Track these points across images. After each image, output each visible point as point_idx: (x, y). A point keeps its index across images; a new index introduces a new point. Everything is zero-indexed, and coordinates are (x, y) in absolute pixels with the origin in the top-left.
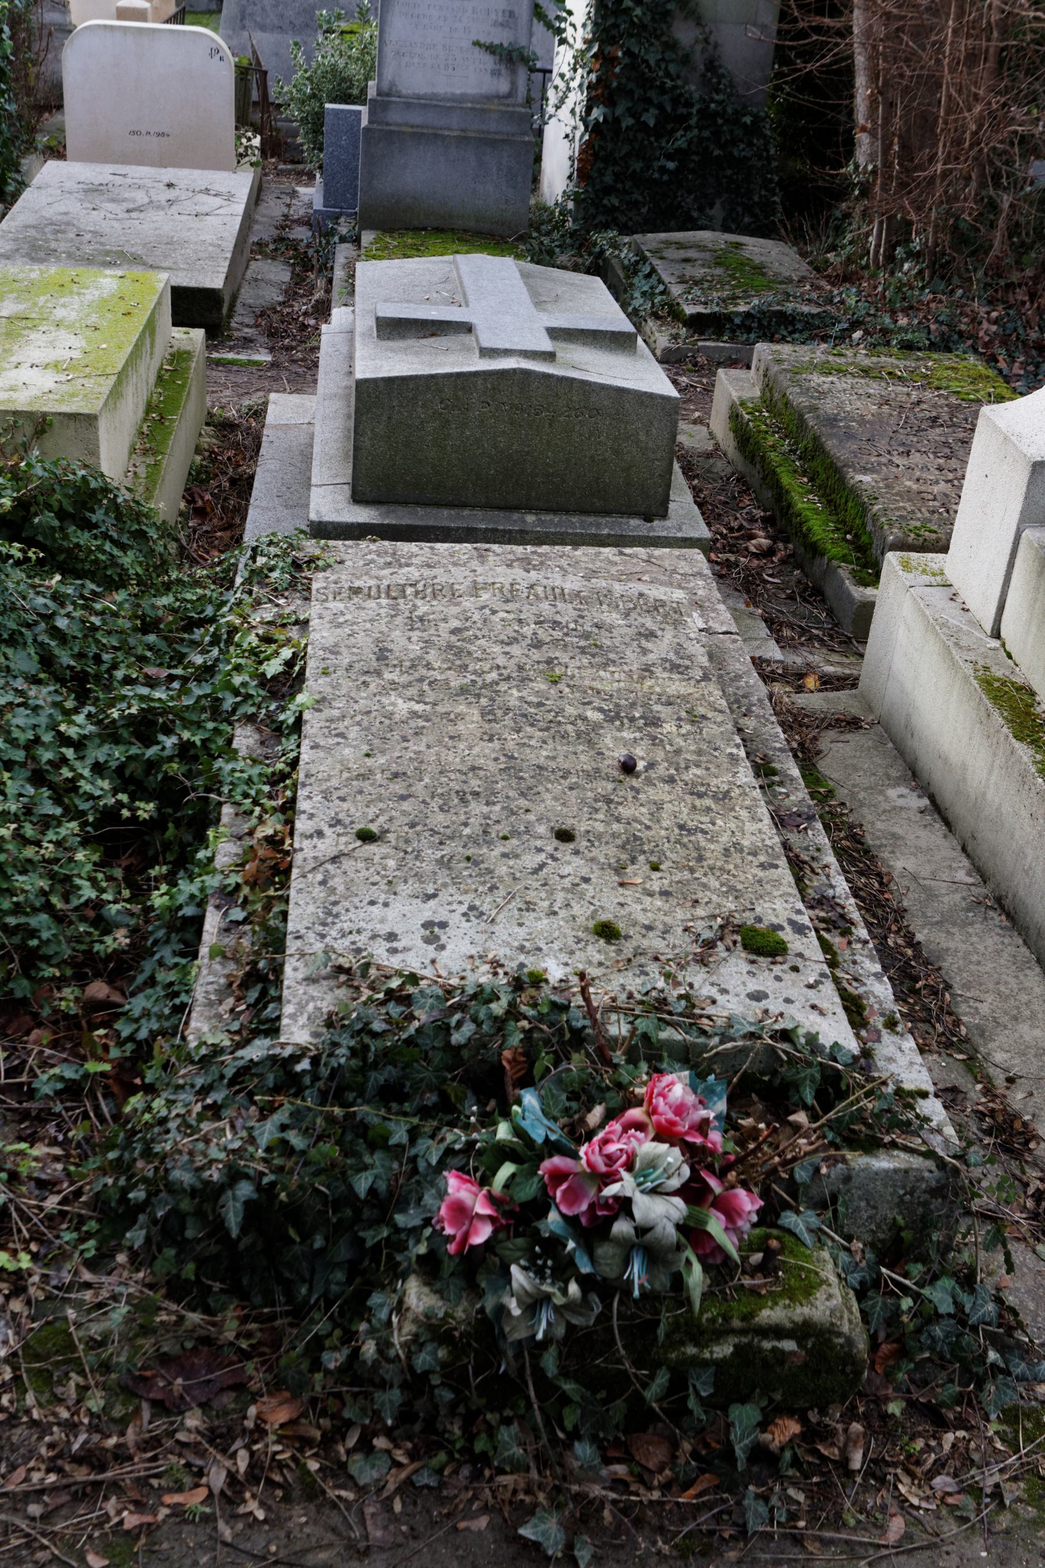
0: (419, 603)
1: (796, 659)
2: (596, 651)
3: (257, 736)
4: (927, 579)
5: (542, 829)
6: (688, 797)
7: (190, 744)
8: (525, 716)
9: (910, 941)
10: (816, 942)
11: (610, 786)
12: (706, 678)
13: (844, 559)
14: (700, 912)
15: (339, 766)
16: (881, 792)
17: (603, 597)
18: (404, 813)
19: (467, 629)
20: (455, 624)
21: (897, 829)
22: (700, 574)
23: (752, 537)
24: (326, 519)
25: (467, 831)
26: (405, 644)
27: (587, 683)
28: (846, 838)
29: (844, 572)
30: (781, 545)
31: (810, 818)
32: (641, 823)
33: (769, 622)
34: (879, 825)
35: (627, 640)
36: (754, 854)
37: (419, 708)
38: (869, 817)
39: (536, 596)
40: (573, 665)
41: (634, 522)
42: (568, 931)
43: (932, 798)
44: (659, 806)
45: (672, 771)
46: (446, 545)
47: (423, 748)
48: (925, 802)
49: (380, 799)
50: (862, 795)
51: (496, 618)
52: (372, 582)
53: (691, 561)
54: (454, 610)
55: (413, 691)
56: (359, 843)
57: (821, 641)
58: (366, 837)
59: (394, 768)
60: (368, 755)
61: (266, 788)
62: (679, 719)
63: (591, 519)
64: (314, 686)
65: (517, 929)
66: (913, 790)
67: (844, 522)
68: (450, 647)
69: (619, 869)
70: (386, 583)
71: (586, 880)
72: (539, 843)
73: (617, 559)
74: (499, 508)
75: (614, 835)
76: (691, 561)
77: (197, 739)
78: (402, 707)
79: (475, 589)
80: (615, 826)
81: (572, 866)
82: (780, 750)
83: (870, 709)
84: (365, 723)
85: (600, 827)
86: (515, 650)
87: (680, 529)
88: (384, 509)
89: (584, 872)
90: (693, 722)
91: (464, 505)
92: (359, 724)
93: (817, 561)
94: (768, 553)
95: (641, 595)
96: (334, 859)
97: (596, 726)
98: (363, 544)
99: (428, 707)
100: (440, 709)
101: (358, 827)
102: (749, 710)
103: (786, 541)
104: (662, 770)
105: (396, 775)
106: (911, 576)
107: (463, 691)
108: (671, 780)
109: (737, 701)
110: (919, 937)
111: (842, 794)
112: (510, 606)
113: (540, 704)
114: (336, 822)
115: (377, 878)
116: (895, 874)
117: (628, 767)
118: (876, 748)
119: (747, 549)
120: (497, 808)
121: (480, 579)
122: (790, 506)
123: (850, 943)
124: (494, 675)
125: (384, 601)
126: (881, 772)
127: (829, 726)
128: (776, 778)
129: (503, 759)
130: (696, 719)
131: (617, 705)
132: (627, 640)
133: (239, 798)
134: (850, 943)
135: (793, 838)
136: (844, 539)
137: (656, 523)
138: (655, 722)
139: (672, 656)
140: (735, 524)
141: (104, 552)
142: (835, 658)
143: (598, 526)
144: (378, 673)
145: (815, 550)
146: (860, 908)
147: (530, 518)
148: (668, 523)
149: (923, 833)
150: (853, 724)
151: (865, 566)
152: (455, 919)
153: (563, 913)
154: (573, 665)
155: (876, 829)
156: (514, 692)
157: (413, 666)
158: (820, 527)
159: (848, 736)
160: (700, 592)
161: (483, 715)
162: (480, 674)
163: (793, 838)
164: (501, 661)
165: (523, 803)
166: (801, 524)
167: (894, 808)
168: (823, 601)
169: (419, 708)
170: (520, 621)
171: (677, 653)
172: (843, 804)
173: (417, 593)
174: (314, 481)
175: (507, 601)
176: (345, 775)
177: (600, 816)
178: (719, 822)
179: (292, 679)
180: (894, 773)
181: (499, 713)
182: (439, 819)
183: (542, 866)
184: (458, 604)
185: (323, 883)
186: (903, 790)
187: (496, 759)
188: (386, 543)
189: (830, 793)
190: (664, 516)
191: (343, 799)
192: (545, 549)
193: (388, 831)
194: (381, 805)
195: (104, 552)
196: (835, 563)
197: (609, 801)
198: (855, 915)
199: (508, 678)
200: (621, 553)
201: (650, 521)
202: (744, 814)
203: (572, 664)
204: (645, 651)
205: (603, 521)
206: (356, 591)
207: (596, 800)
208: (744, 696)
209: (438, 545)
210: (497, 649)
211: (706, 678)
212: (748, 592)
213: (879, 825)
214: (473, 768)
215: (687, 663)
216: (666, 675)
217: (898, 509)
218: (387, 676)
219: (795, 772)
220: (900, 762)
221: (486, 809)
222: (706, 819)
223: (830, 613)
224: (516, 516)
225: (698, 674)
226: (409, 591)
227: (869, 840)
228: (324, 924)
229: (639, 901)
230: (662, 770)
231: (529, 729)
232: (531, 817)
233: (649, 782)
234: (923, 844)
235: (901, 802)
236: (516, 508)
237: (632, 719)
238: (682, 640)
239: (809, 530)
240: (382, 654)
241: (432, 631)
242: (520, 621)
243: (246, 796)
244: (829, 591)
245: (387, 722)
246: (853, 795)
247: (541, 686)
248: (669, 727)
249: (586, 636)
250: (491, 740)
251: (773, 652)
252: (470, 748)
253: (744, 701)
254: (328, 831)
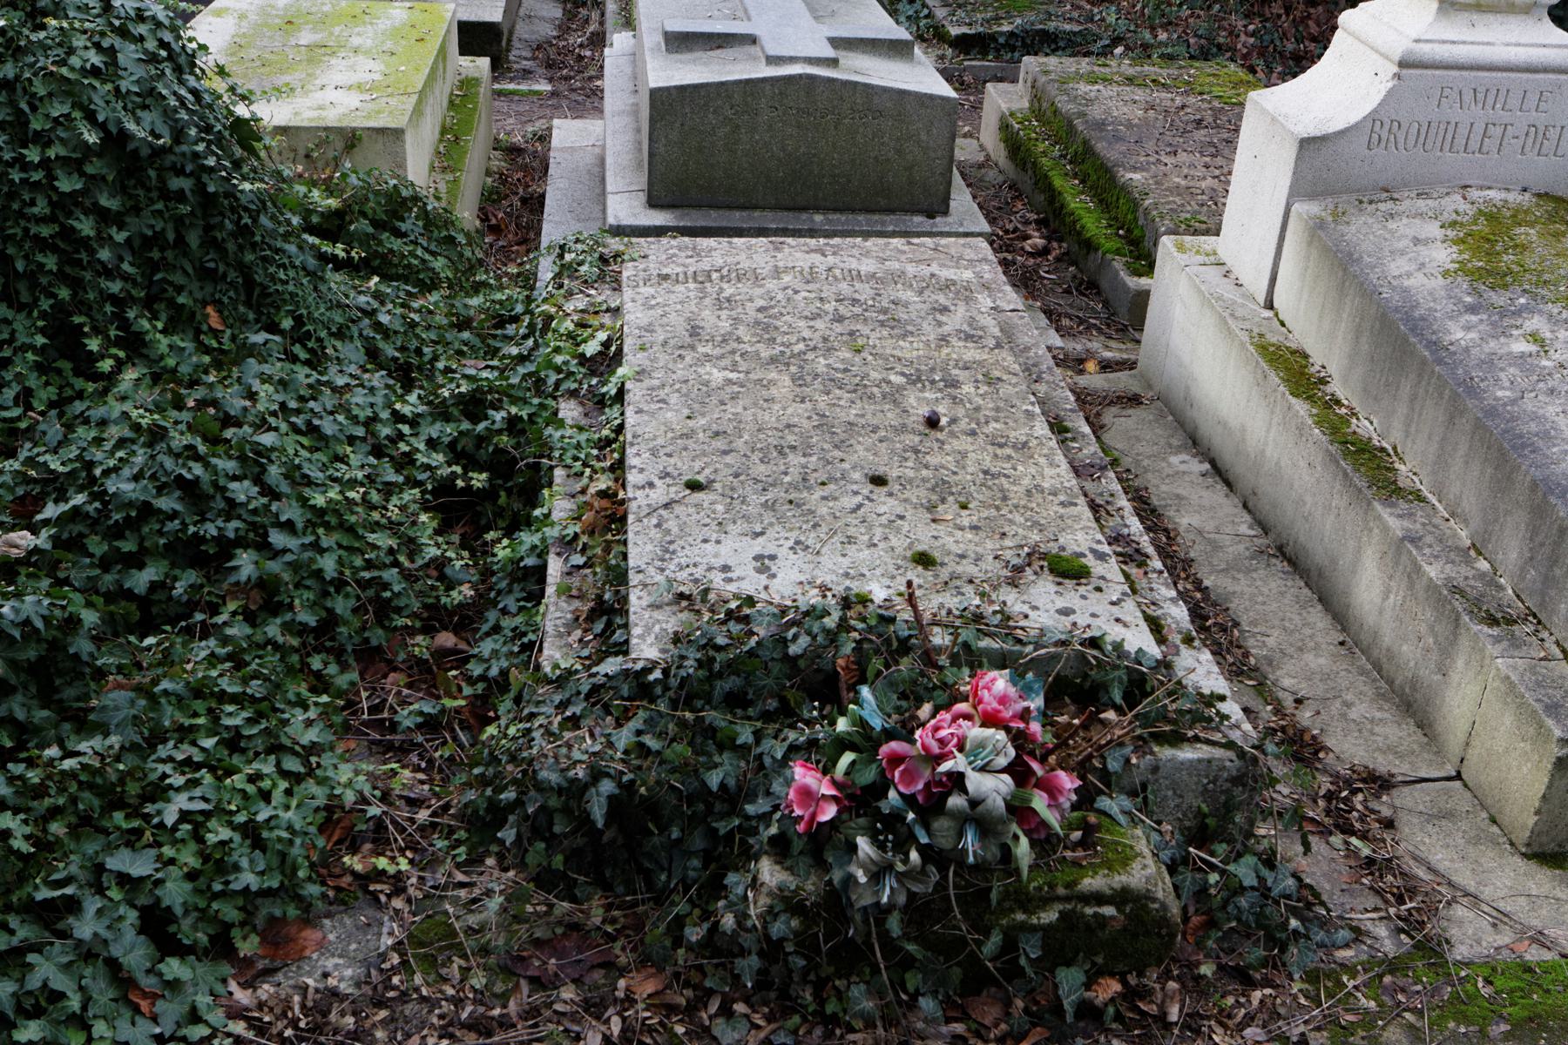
0: (725, 286)
1: (1076, 346)
3: (580, 409)
4: (1201, 259)
5: (857, 476)
6: (989, 447)
12: (998, 346)
13: (1118, 252)
14: (1008, 543)
15: (663, 428)
17: (898, 277)
18: (727, 465)
19: (772, 307)
20: (762, 303)
21: (1180, 491)
22: (985, 260)
23: (1027, 237)
24: (624, 223)
25: (787, 479)
26: (715, 321)
27: (888, 351)
29: (1118, 264)
30: (1055, 245)
31: (1103, 468)
33: (1048, 313)
35: (923, 314)
36: (1055, 494)
38: (1154, 481)
39: (835, 277)
40: (874, 336)
41: (918, 219)
43: (1213, 463)
44: (964, 455)
45: (974, 426)
46: (743, 240)
47: (739, 409)
48: (1207, 466)
49: (704, 454)
51: (798, 297)
52: (679, 270)
53: (976, 249)
54: (758, 291)
55: (726, 362)
57: (1099, 330)
58: (694, 486)
59: (715, 427)
61: (595, 452)
63: (876, 217)
65: (841, 559)
66: (1194, 456)
67: (1116, 218)
68: (757, 323)
70: (692, 269)
71: (902, 517)
72: (855, 487)
73: (906, 248)
74: (789, 209)
75: (923, 480)
76: (976, 249)
77: (524, 414)
78: (717, 376)
79: (777, 273)
80: (924, 472)
81: (886, 505)
83: (1150, 387)
84: (684, 390)
85: (911, 473)
86: (819, 324)
87: (962, 225)
88: (678, 212)
89: (899, 510)
91: (755, 207)
92: (678, 391)
93: (1092, 256)
94: (1043, 252)
95: (933, 275)
96: (666, 506)
98: (664, 240)
99: (742, 376)
103: (1060, 240)
104: (963, 424)
105: (717, 434)
106: (1185, 256)
107: (773, 360)
108: (973, 433)
110: (1206, 583)
112: (811, 287)
113: (846, 370)
114: (665, 475)
115: (707, 521)
116: (1181, 530)
117: (932, 422)
118: (1156, 421)
119: (1022, 249)
120: (814, 459)
121: (781, 264)
122: (1062, 206)
123: (1146, 573)
124: (801, 346)
125: (692, 285)
126: (1162, 442)
127: (1111, 403)
130: (991, 381)
131: (918, 370)
132: (923, 314)
133: (569, 461)
134: (1146, 573)
136: (1117, 234)
137: (938, 219)
138: (954, 384)
139: (965, 327)
140: (1010, 227)
141: (417, 257)
142: (1113, 344)
143: (883, 223)
144: (693, 348)
145: (1089, 246)
147: (818, 218)
148: (949, 219)
149: (1205, 493)
150: (1134, 400)
151: (1138, 258)
153: (882, 545)
154: (874, 336)
155: (1160, 491)
157: (724, 341)
158: (1093, 223)
159: (1130, 412)
160: (986, 276)
161: (793, 381)
163: (1089, 485)
164: (806, 334)
165: (837, 453)
166: (1074, 222)
168: (1099, 293)
170: (821, 299)
171: (970, 325)
172: (1128, 470)
173: (722, 278)
174: (609, 188)
175: (808, 282)
176: (670, 435)
177: (910, 464)
178: (1020, 468)
179: (610, 357)
181: (808, 379)
183: (859, 506)
184: (762, 286)
185: (658, 526)
187: (809, 418)
188: (686, 239)
190: (946, 213)
191: (669, 455)
192: (836, 241)
195: (417, 257)
196: (1109, 256)
197: (916, 452)
199: (815, 348)
200: (909, 243)
201: (933, 217)
202: (1042, 461)
203: (873, 335)
204: (940, 324)
205: (887, 218)
206: (666, 277)
209: (735, 240)
210: (802, 323)
211: (998, 346)
212: (1026, 287)
213: (1164, 488)
214: (788, 426)
215: (980, 333)
216: (961, 344)
217: (1168, 203)
218: (701, 349)
219: (1087, 429)
221: (803, 460)
223: (1106, 304)
224: (804, 216)
225: (992, 343)
226: (715, 276)
227: (1155, 501)
228: (663, 560)
229: (951, 534)
230: (963, 424)
232: (846, 466)
233: (953, 434)
234: (1206, 502)
235: (1183, 467)
236: (804, 209)
237: (933, 382)
238: (975, 313)
239: (1083, 227)
240: (694, 331)
241: (740, 310)
242: (821, 299)
244: (1104, 284)
246: (1138, 462)
247: (846, 354)
248: (967, 389)
249: (885, 311)
250: (803, 401)
252: (784, 409)
253: (1035, 369)
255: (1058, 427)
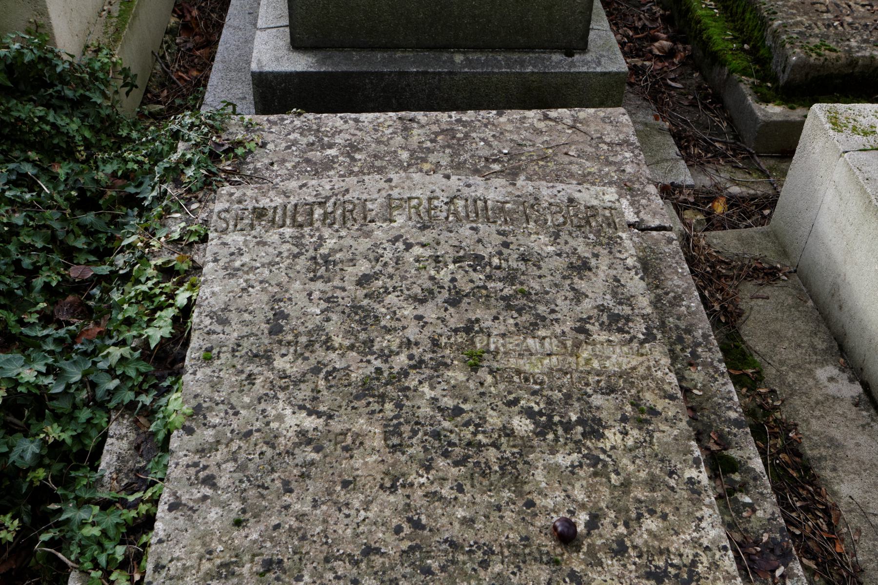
0: (326, 232)
1: (705, 181)
2: (525, 307)
3: (132, 436)
4: (859, 140)
8: (437, 435)
12: (649, 337)
13: (744, 72)
16: (810, 372)
17: (528, 210)
19: (376, 276)
20: (364, 267)
21: (837, 434)
22: (626, 143)
23: (656, 39)
24: (266, 69)
26: (305, 307)
27: (513, 363)
28: (783, 450)
29: (746, 85)
30: (680, 46)
31: (785, 557)
33: (680, 138)
34: (815, 425)
35: (558, 278)
38: (804, 412)
39: (456, 214)
40: (498, 332)
41: (557, 57)
43: (866, 386)
45: (622, 529)
46: (371, 116)
47: (307, 508)
48: (857, 389)
50: (791, 377)
51: (409, 257)
52: (279, 201)
53: (615, 124)
54: (364, 244)
55: (304, 392)
57: (725, 156)
59: (269, 550)
60: (238, 523)
61: (120, 552)
62: (624, 419)
63: (516, 56)
64: (195, 378)
67: (741, 31)
68: (355, 308)
70: (293, 200)
73: (541, 125)
74: (430, 48)
76: (615, 124)
77: (66, 436)
78: (291, 421)
79: (391, 206)
82: (737, 423)
83: (784, 253)
84: (242, 456)
86: (430, 312)
87: (599, 63)
88: (320, 55)
90: (641, 423)
91: (396, 48)
93: (717, 69)
94: (670, 54)
95: (571, 200)
97: (525, 446)
98: (288, 118)
100: (336, 426)
102: (694, 354)
103: (685, 42)
104: (610, 530)
106: (842, 137)
107: (366, 389)
108: (619, 550)
109: (680, 340)
111: (770, 372)
112: (427, 236)
113: (457, 411)
116: (843, 506)
118: (796, 307)
119: (651, 51)
121: (395, 193)
122: (689, 10)
124: (401, 360)
125: (288, 231)
127: (749, 277)
128: (737, 477)
129: (407, 529)
130: (644, 416)
131: (550, 402)
132: (558, 278)
133: (88, 565)
136: (743, 49)
137: (577, 57)
138: (594, 428)
139: (609, 301)
140: (639, 24)
141: (48, 123)
142: (740, 176)
143: (522, 63)
144: (267, 358)
145: (716, 59)
147: (459, 58)
148: (588, 57)
149: (862, 438)
150: (771, 274)
151: (764, 79)
154: (498, 332)
157: (310, 345)
158: (721, 37)
159: (767, 290)
160: (629, 169)
161: (386, 437)
162: (386, 356)
164: (412, 332)
166: (701, 31)
167: (827, 397)
168: (723, 108)
169: (310, 423)
170: (437, 259)
171: (614, 294)
172: (773, 391)
173: (326, 215)
174: (260, 24)
175: (424, 227)
176: (206, 566)
180: (821, 346)
181: (406, 429)
184: (368, 234)
186: (831, 370)
187: (398, 530)
188: (311, 116)
189: (759, 377)
190: (583, 48)
192: (469, 115)
195: (48, 123)
196: (736, 76)
199: (419, 364)
200: (546, 118)
201: (570, 54)
203: (498, 328)
204: (578, 296)
205: (526, 57)
206: (260, 213)
208: (688, 331)
209: (363, 116)
210: (408, 311)
211: (649, 337)
212: (656, 102)
213: (815, 425)
214: (369, 551)
215: (627, 310)
216: (603, 337)
217: (797, 24)
218: (280, 363)
219: (757, 464)
220: (823, 327)
223: (730, 121)
224: (445, 56)
225: (639, 328)
226: (318, 212)
230: (610, 530)
231: (441, 463)
234: (865, 456)
235: (832, 389)
236: (445, 48)
237: (568, 427)
238: (619, 271)
239: (709, 38)
240: (277, 323)
241: (337, 282)
242: (437, 259)
243: (94, 560)
244: (729, 101)
245: (269, 452)
246: (781, 376)
247: (457, 375)
248: (612, 437)
249: (511, 278)
250: (393, 489)
251: (684, 176)
255: (720, 465)
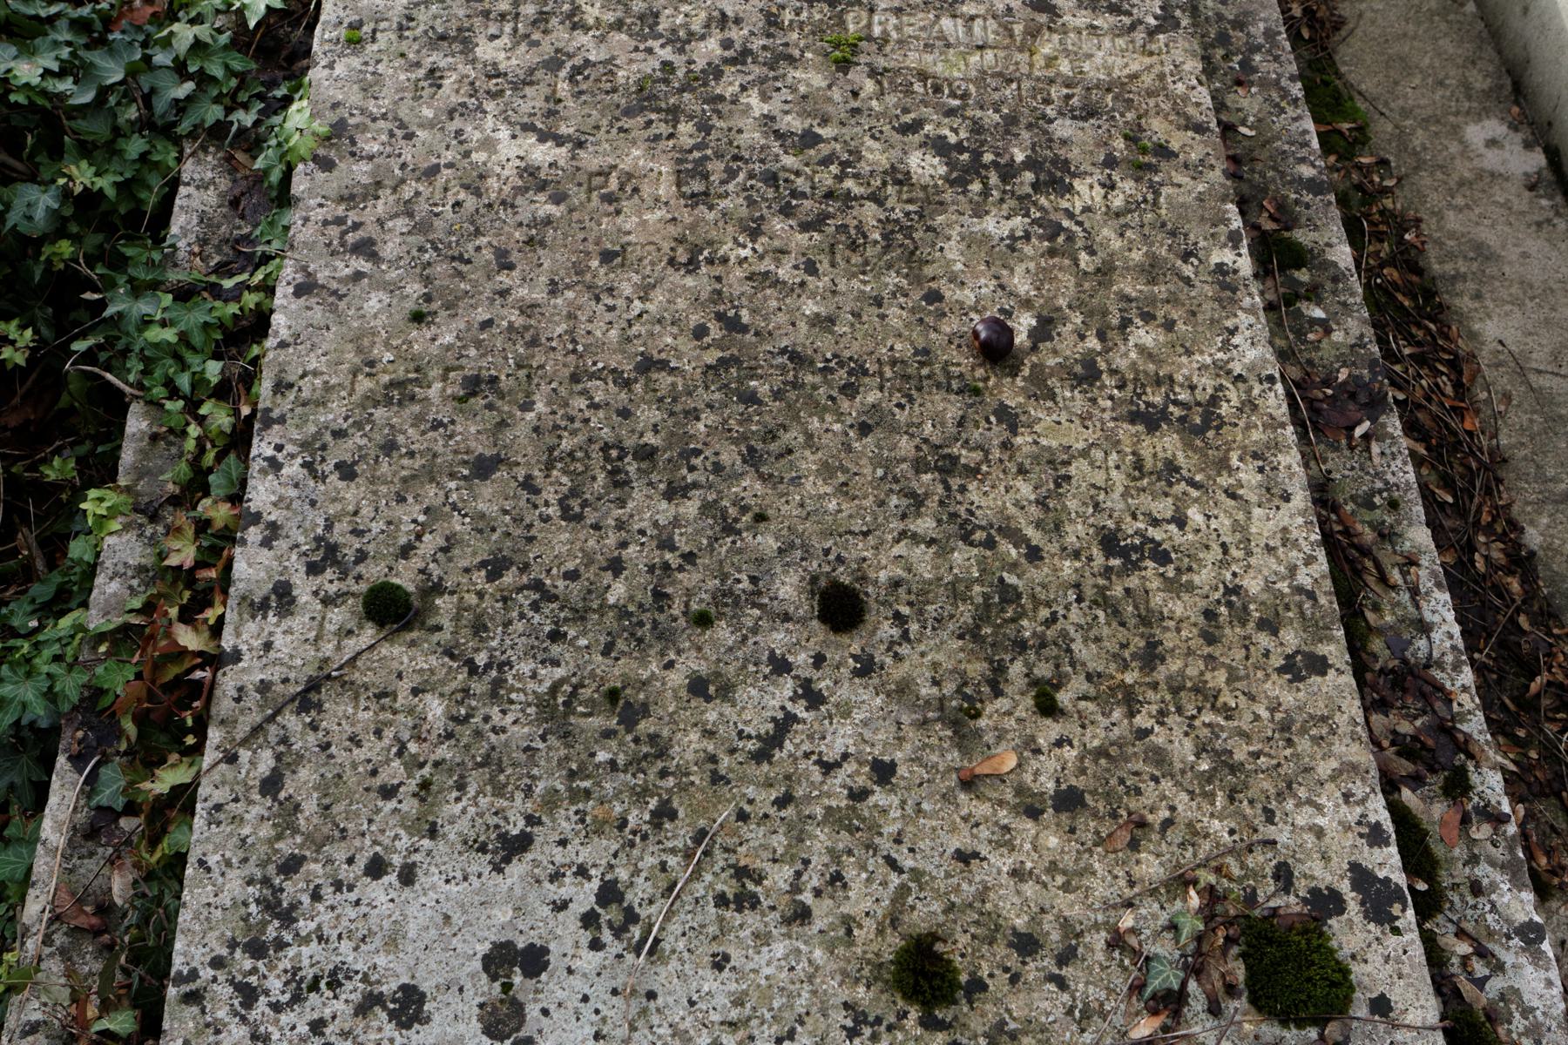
3: (224, 183)
5: (788, 588)
6: (1126, 431)
7: (90, 198)
8: (772, 179)
9: (1522, 562)
10: (1417, 951)
11: (952, 409)
14: (1151, 867)
15: (351, 356)
16: (1456, 131)
18: (483, 524)
21: (1489, 236)
25: (618, 592)
27: (913, 59)
28: (1391, 262)
31: (1375, 406)
32: (1017, 538)
34: (1453, 221)
36: (1270, 625)
37: (543, 154)
38: (1435, 199)
42: (833, 988)
43: (1552, 154)
44: (1057, 465)
45: (1093, 343)
47: (539, 295)
48: (1537, 160)
49: (430, 474)
50: (1419, 138)
55: (532, 101)
56: (369, 634)
58: (390, 610)
59: (474, 361)
60: (418, 318)
61: (213, 370)
62: (1110, 162)
64: (330, 76)
65: (709, 982)
66: (1514, 128)
69: (961, 720)
71: (884, 772)
72: (778, 639)
75: (957, 592)
77: (105, 183)
78: (509, 151)
80: (963, 557)
81: (857, 723)
82: (1314, 186)
84: (422, 208)
85: (923, 561)
89: (880, 743)
90: (1140, 170)
92: (408, 210)
96: (307, 699)
97: (930, 202)
99: (563, 152)
100: (590, 160)
101: (374, 572)
102: (1246, 65)
104: (1069, 345)
105: (474, 385)
107: (644, 97)
108: (1087, 375)
109: (1223, 39)
110: (1533, 538)
111: (1382, 129)
113: (809, 139)
114: (325, 556)
115: (394, 771)
116: (1484, 358)
117: (996, 350)
120: (690, 508)
123: (1465, 820)
124: (709, 49)
126: (1453, 76)
128: (1303, 276)
129: (715, 331)
130: (1147, 159)
131: (977, 128)
133: (159, 391)
134: (1465, 820)
135: (1339, 465)
138: (1054, 175)
144: (462, 40)
146: (1418, 461)
149: (1534, 245)
152: (564, 937)
153: (824, 914)
156: (753, 99)
157: (542, 18)
161: (680, 179)
162: (681, 40)
163: (1339, 465)
165: (750, 487)
167: (1480, 174)
169: (543, 154)
172: (1383, 163)
176: (364, 384)
177: (925, 525)
178: (1195, 515)
180: (1480, 83)
181: (716, 168)
182: (560, 545)
183: (785, 724)
185: (271, 785)
186: (1494, 127)
187: (700, 332)
189: (1361, 136)
191: (347, 471)
193: (438, 589)
194: (431, 493)
197: (947, 466)
198: (1475, 726)
199: (743, 57)
202: (1248, 475)
207: (919, 466)
208: (1239, 24)
213: (1453, 221)
214: (648, 365)
216: (1082, 19)
218: (486, 51)
219: (1343, 255)
220: (1489, 51)
221: (665, 511)
222: (1163, 508)
227: (1436, 266)
228: (257, 949)
229: (1005, 840)
230: (1069, 345)
231: (778, 225)
232: (768, 542)
233: (1041, 390)
234: (1535, 274)
235: (1492, 159)
237: (1008, 172)
243: (170, 384)
245: (470, 202)
246: (1402, 136)
247: (811, 77)
248: (1087, 192)
250: (692, 266)
252: (645, 292)
253: (1238, 37)
254: (303, 588)
255: (1277, 254)
